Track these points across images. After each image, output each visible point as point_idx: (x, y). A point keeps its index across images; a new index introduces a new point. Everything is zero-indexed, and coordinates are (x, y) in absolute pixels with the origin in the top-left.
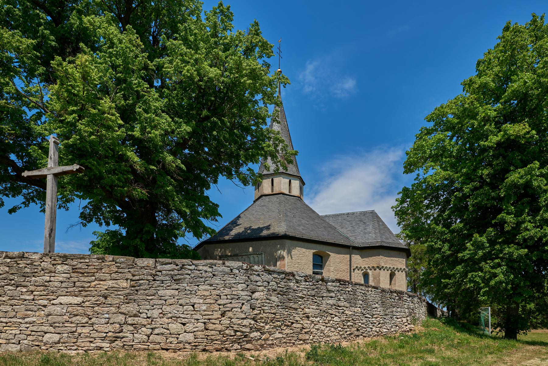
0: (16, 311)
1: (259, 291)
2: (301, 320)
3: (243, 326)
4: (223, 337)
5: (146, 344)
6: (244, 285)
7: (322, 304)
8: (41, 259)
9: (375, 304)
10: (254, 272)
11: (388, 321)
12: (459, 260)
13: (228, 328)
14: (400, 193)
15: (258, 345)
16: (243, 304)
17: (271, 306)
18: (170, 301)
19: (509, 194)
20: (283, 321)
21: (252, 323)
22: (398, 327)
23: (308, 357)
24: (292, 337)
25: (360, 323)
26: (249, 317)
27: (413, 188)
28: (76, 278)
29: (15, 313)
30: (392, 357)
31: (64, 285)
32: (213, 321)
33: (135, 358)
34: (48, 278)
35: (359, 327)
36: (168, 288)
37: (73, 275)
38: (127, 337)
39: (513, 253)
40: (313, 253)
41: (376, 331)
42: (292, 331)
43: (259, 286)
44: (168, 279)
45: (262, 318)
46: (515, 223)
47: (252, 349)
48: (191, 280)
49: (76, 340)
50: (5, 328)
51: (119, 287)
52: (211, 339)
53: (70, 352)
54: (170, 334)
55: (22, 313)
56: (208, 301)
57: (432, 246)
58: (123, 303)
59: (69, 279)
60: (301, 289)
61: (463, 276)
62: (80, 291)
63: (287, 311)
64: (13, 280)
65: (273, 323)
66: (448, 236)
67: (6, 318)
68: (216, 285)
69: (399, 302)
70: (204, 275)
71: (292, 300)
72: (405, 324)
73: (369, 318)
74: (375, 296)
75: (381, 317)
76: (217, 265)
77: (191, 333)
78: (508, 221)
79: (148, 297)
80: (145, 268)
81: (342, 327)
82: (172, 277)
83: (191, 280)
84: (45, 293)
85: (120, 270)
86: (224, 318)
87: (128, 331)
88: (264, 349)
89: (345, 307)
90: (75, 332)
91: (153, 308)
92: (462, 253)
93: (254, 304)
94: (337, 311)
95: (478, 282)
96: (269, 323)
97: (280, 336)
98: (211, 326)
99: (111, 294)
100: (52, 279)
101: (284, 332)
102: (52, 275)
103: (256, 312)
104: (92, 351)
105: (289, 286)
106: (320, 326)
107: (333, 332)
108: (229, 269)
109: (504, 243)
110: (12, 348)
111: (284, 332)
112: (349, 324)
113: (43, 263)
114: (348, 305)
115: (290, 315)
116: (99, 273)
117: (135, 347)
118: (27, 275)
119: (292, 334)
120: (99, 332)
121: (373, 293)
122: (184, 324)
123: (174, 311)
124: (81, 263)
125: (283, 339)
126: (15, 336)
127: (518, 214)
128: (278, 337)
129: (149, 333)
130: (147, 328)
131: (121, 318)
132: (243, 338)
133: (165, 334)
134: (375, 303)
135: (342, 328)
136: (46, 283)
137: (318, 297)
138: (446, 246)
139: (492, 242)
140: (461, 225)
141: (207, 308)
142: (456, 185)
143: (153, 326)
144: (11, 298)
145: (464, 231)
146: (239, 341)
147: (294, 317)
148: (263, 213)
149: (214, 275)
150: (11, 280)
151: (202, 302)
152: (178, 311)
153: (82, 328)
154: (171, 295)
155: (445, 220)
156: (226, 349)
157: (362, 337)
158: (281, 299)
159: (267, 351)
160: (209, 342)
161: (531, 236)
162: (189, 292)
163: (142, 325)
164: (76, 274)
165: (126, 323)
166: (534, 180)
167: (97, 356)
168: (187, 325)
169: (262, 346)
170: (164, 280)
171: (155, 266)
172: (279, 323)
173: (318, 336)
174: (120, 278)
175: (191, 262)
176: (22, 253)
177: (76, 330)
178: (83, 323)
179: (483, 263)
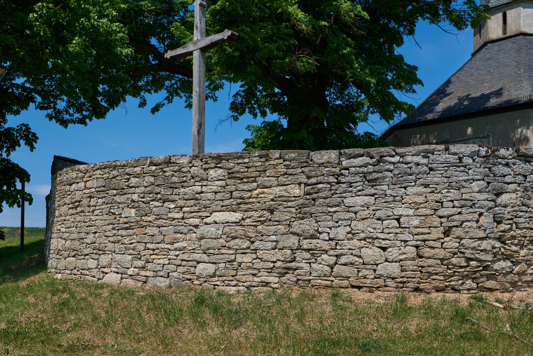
0: (163, 234)
1: (509, 192)
3: (481, 251)
4: (448, 268)
5: (329, 278)
6: (482, 182)
8: (191, 163)
13: (455, 254)
15: (507, 282)
16: (481, 214)
17: (530, 217)
18: (361, 213)
21: (496, 246)
26: (492, 235)
28: (233, 187)
29: (162, 237)
31: (218, 196)
32: (431, 243)
33: (315, 299)
34: (198, 189)
36: (359, 193)
37: (229, 182)
38: (302, 268)
44: (358, 179)
45: (513, 237)
47: (497, 290)
48: (395, 179)
49: (235, 271)
50: (152, 257)
51: (289, 195)
52: (428, 272)
53: (228, 288)
54: (364, 264)
55: (171, 236)
56: (422, 211)
58: (296, 218)
59: (224, 187)
62: (239, 204)
64: (159, 193)
67: (152, 243)
68: (434, 186)
77: (396, 262)
79: (329, 209)
80: (325, 165)
82: (365, 177)
83: (395, 179)
84: (196, 208)
85: (290, 171)
86: (450, 238)
87: (303, 259)
88: (518, 290)
90: (234, 261)
91: (337, 225)
93: (499, 214)
96: (526, 246)
98: (427, 252)
99: (279, 207)
100: (204, 189)
102: (204, 184)
103: (503, 227)
104: (256, 288)
110: (160, 282)
113: (192, 168)
116: (263, 177)
117: (313, 282)
118: (174, 186)
120: (264, 261)
122: (384, 249)
123: (369, 229)
124: (238, 164)
126: (163, 267)
129: (332, 262)
130: (330, 256)
131: (293, 241)
133: (356, 263)
136: (197, 196)
141: (421, 223)
143: (339, 252)
144: (158, 217)
150: (157, 194)
151: (412, 214)
152: (375, 229)
153: (242, 255)
154: (363, 204)
159: (525, 293)
160: (425, 277)
162: (391, 199)
163: (323, 251)
164: (233, 181)
165: (300, 248)
167: (262, 295)
168: (389, 250)
169: (514, 284)
170: (353, 181)
171: (340, 160)
174: (290, 183)
176: (168, 157)
177: (235, 258)
178: (244, 249)
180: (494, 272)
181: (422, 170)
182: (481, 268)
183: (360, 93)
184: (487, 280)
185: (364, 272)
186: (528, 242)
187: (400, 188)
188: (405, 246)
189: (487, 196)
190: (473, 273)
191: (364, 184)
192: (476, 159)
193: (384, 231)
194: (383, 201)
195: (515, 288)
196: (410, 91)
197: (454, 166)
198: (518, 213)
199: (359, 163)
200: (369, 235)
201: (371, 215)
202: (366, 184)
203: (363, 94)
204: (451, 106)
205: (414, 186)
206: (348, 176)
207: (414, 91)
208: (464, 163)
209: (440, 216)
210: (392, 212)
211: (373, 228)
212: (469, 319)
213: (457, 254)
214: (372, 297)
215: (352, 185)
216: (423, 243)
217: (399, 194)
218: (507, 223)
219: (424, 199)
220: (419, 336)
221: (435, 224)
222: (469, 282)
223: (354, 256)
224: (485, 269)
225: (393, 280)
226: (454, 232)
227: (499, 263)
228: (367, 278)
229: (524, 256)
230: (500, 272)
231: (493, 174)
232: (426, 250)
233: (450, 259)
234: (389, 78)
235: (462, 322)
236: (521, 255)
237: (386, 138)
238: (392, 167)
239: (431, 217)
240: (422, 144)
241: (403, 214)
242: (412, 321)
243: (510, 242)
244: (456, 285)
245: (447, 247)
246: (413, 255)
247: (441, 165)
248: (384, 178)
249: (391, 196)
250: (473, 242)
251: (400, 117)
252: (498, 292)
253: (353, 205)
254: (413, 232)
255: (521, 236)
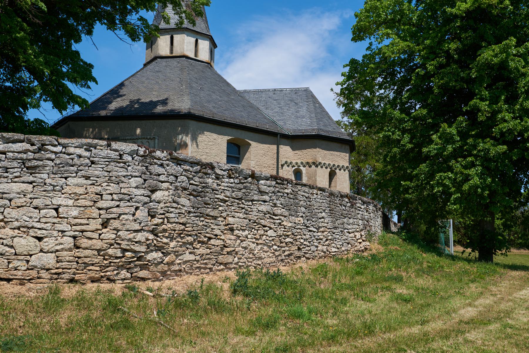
1: (163, 190)
2: (221, 234)
3: (136, 242)
4: (104, 259)
6: (139, 179)
7: (252, 211)
9: (321, 212)
10: (155, 161)
11: (338, 236)
12: (423, 156)
13: (111, 245)
14: (347, 65)
15: (158, 272)
16: (137, 208)
17: (179, 213)
18: (17, 200)
19: (481, 75)
20: (196, 235)
21: (150, 238)
22: (350, 245)
23: (234, 290)
24: (209, 259)
25: (302, 238)
27: (363, 60)
30: (350, 288)
32: (89, 234)
35: (301, 245)
36: (16, 180)
39: (489, 150)
40: (228, 140)
41: (323, 251)
42: (209, 251)
43: (162, 182)
44: (16, 165)
45: (165, 231)
46: (490, 113)
47: (149, 279)
48: (56, 168)
52: (84, 263)
54: (16, 254)
56: (82, 202)
57: (388, 137)
60: (223, 188)
61: (428, 178)
63: (203, 221)
65: (182, 238)
66: (408, 125)
68: (95, 179)
69: (351, 210)
70: (76, 161)
71: (209, 204)
72: (359, 241)
73: (314, 232)
74: (321, 201)
75: (330, 230)
76: (98, 147)
77: (52, 252)
78: (483, 108)
81: (278, 244)
82: (24, 163)
86: (107, 230)
88: (167, 279)
89: (283, 216)
92: (426, 147)
93: (153, 208)
94: (272, 221)
95: (448, 185)
96: (175, 239)
97: (192, 257)
98: (84, 242)
101: (198, 252)
103: (156, 221)
105: (206, 183)
106: (249, 243)
107: (266, 252)
108: (117, 153)
109: (475, 137)
111: (198, 252)
112: (288, 240)
114: (287, 214)
115: (206, 226)
119: (209, 254)
121: (319, 197)
122: (40, 239)
125: (195, 262)
127: (494, 100)
128: (188, 259)
132: (135, 261)
134: (321, 210)
135: (278, 246)
137: (246, 201)
138: (407, 138)
139: (464, 135)
140: (425, 112)
141: (80, 214)
142: (418, 60)
145: (428, 119)
146: (128, 266)
147: (212, 229)
148: (157, 82)
149: (93, 163)
151: (71, 204)
152: (31, 217)
154: (19, 191)
155: (403, 104)
156: (108, 279)
157: (304, 258)
158: (194, 203)
159: (172, 281)
161: (510, 129)
162: (51, 188)
166: (512, 60)
168: (45, 240)
172: (190, 239)
173: (246, 258)
175: (57, 141)
179: (453, 161)
180: (147, 263)
181: (84, 162)
182: (136, 259)
183: (33, 78)
184: (141, 270)
185: (15, 263)
186: (177, 235)
187: (60, 178)
188: (62, 237)
189: (144, 192)
190: (128, 263)
191: (22, 170)
192: (135, 157)
193: (41, 220)
194: (42, 189)
195: (165, 277)
196: (85, 86)
197: (115, 162)
198: (169, 209)
199: (18, 149)
200: (23, 224)
201: (27, 203)
202: (24, 171)
203: (35, 81)
204: (123, 106)
205: (75, 177)
206: (4, 161)
207: (89, 87)
208: (124, 160)
209: (99, 208)
210: (51, 201)
211: (28, 217)
212: (121, 308)
213: (113, 245)
214: (22, 290)
215: (8, 170)
216: (81, 233)
217: (59, 184)
218: (160, 217)
219: (84, 190)
220: (68, 330)
221: (95, 215)
222: (124, 272)
223: (4, 246)
224: (139, 259)
225: (47, 271)
226: (112, 224)
227: (151, 254)
228: (19, 270)
229: (173, 248)
230: (152, 262)
231: (149, 172)
232: (84, 241)
233: (106, 250)
234: (64, 70)
235: (114, 312)
236: (171, 246)
237: (58, 128)
238: (53, 156)
239: (90, 208)
240: (94, 138)
241: (62, 204)
242: (64, 314)
243: (162, 234)
244: (111, 275)
245: (104, 238)
246: (70, 245)
247: (103, 159)
248: (45, 166)
249: (51, 185)
250: (129, 234)
251: (74, 109)
252: (150, 281)
253: (8, 192)
254: (71, 223)
255: (171, 230)
